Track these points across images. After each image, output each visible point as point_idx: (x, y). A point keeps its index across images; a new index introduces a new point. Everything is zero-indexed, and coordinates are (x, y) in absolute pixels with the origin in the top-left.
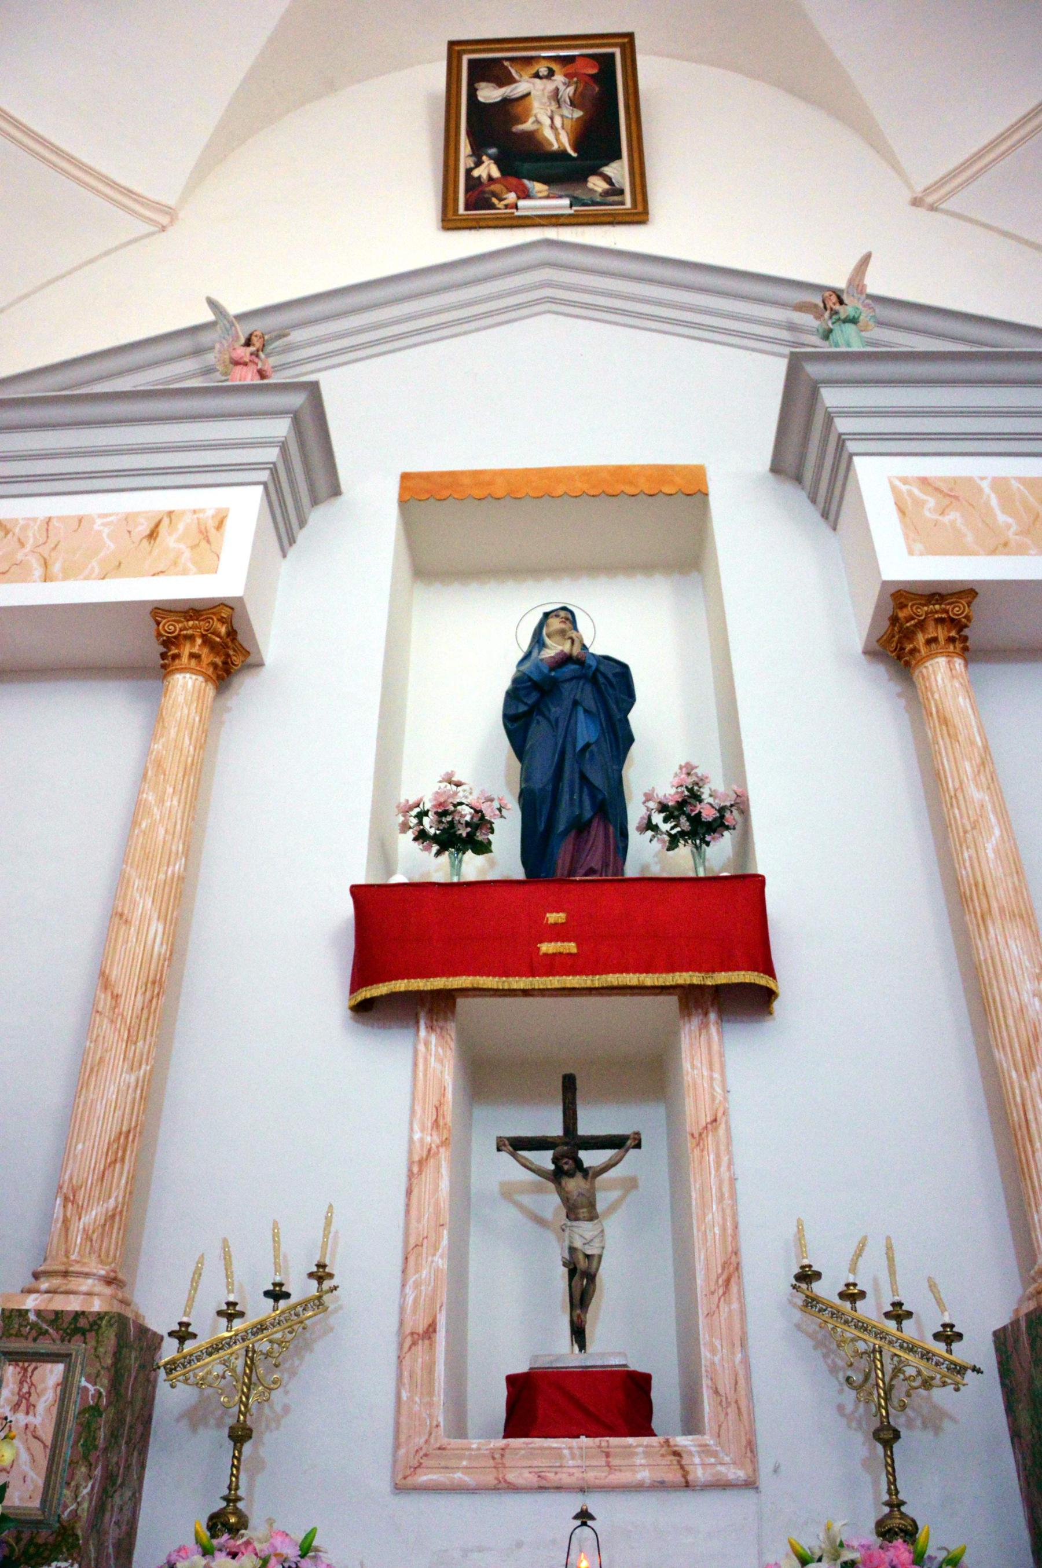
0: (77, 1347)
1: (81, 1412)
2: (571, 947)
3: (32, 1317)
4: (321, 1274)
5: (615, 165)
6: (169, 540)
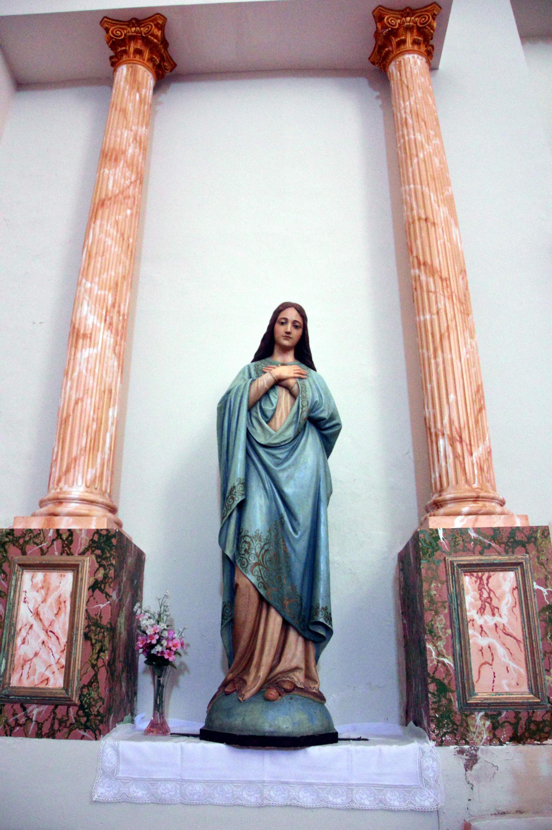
0: (519, 556)
1: (543, 610)
3: (473, 534)
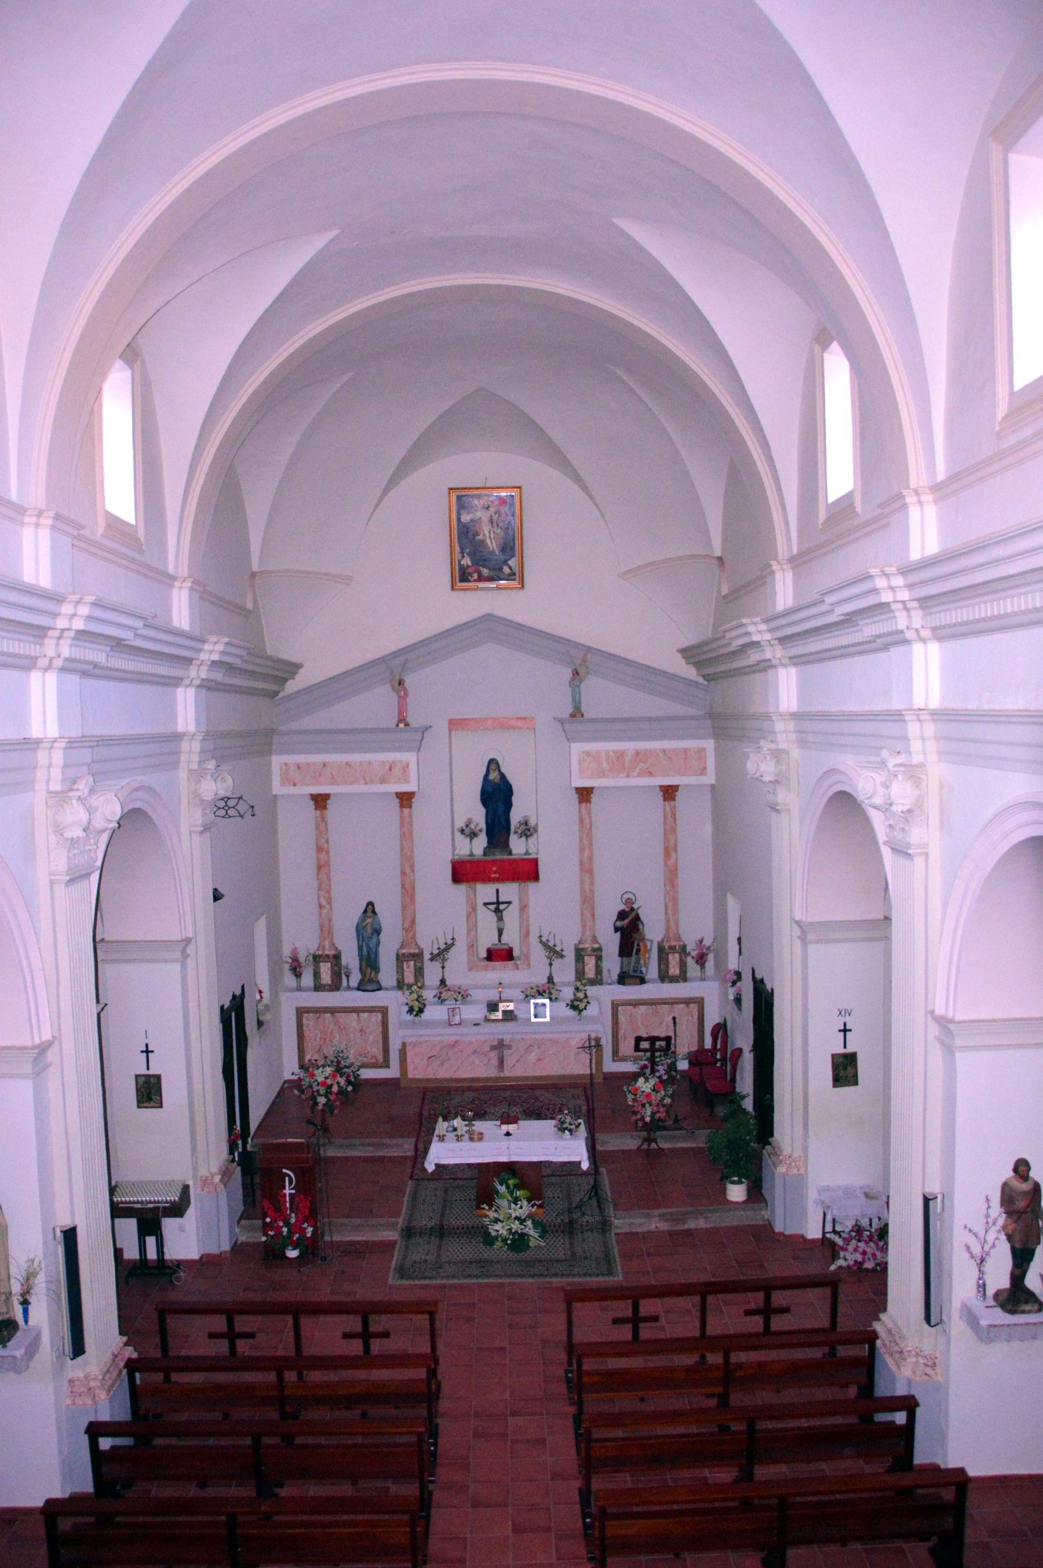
2: (497, 875)
4: (453, 939)
5: (513, 560)
6: (396, 771)
